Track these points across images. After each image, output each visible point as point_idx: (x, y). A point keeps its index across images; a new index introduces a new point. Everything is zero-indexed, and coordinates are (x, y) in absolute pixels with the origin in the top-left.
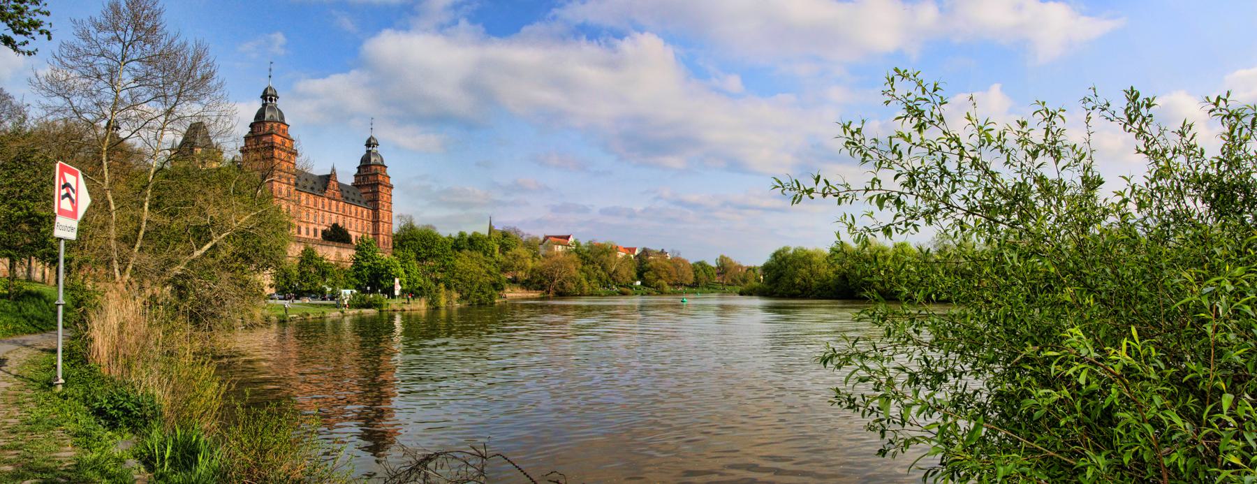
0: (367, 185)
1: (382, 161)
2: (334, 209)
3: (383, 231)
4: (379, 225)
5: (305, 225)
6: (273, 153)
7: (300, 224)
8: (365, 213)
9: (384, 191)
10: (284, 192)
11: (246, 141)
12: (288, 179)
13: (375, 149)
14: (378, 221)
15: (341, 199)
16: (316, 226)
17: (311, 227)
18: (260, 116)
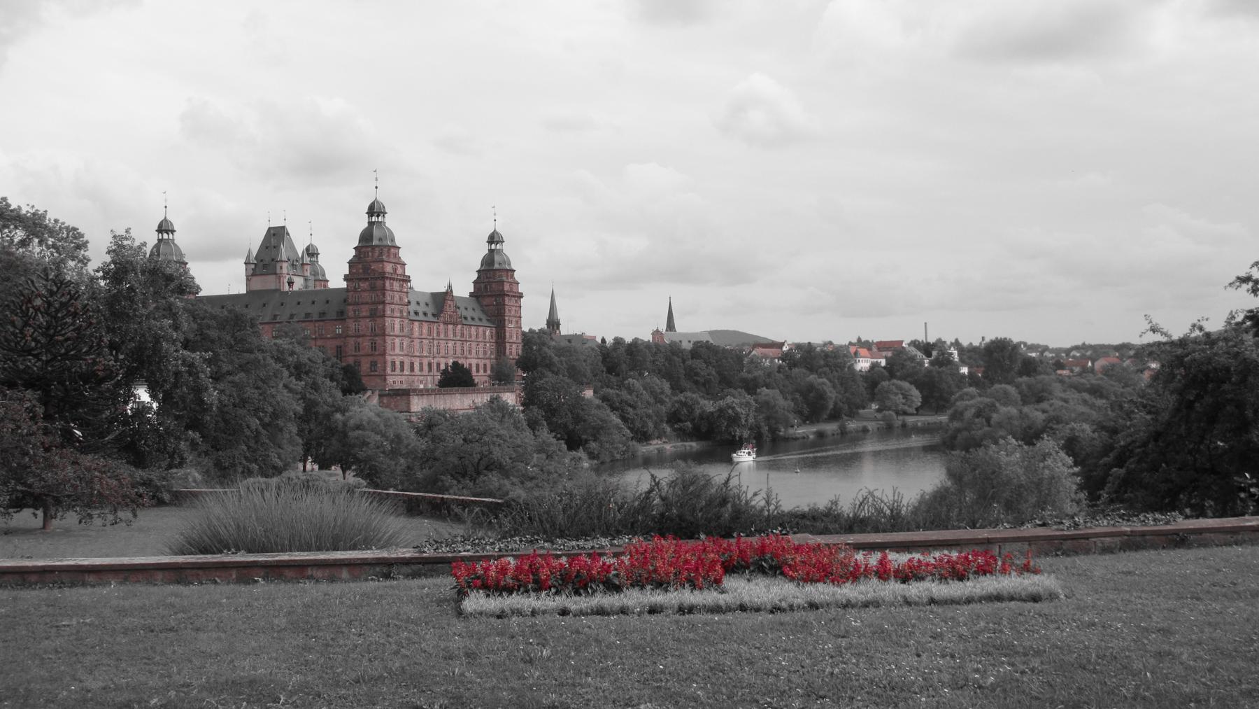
0: (489, 296)
2: (451, 335)
3: (511, 353)
5: (418, 359)
6: (384, 285)
7: (413, 359)
8: (488, 333)
10: (397, 327)
11: (350, 267)
12: (401, 312)
13: (498, 247)
14: (505, 343)
17: (425, 362)
18: (366, 237)
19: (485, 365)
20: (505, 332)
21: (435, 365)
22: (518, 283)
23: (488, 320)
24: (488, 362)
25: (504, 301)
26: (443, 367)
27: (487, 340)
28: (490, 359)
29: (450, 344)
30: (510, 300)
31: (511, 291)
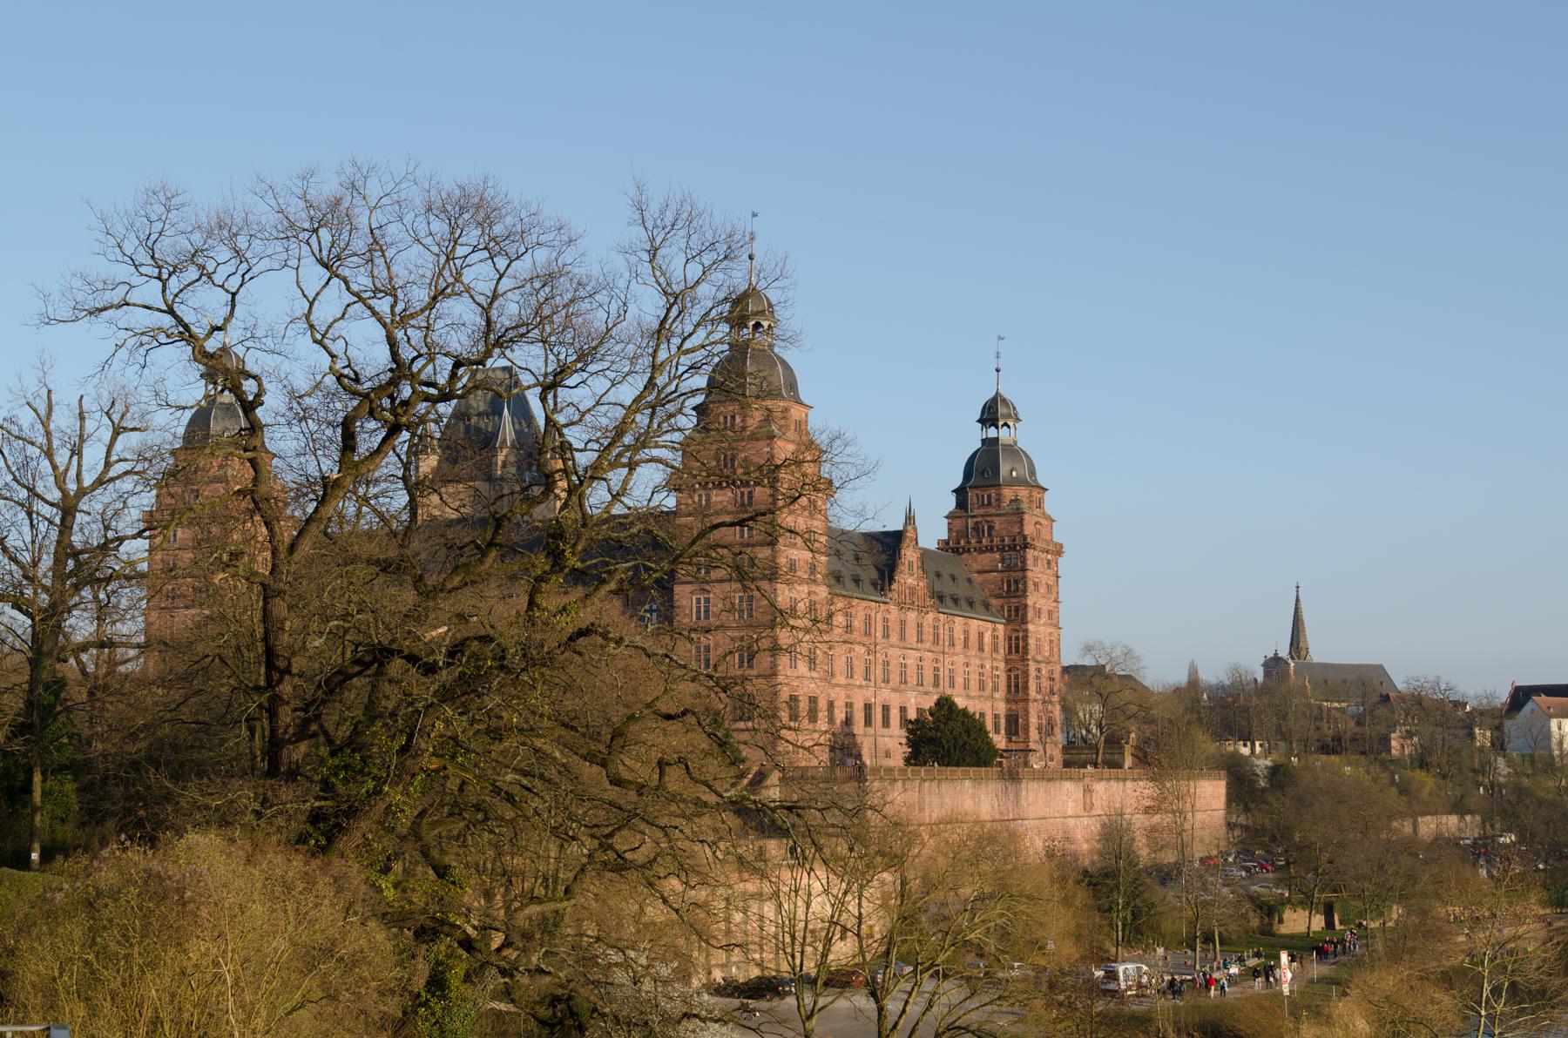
1: (1033, 472)
2: (911, 633)
4: (1026, 674)
8: (987, 638)
14: (1024, 660)
15: (929, 602)
16: (869, 693)
20: (1025, 638)
21: (879, 709)
25: (1024, 561)
26: (912, 715)
29: (911, 659)
30: (1036, 559)
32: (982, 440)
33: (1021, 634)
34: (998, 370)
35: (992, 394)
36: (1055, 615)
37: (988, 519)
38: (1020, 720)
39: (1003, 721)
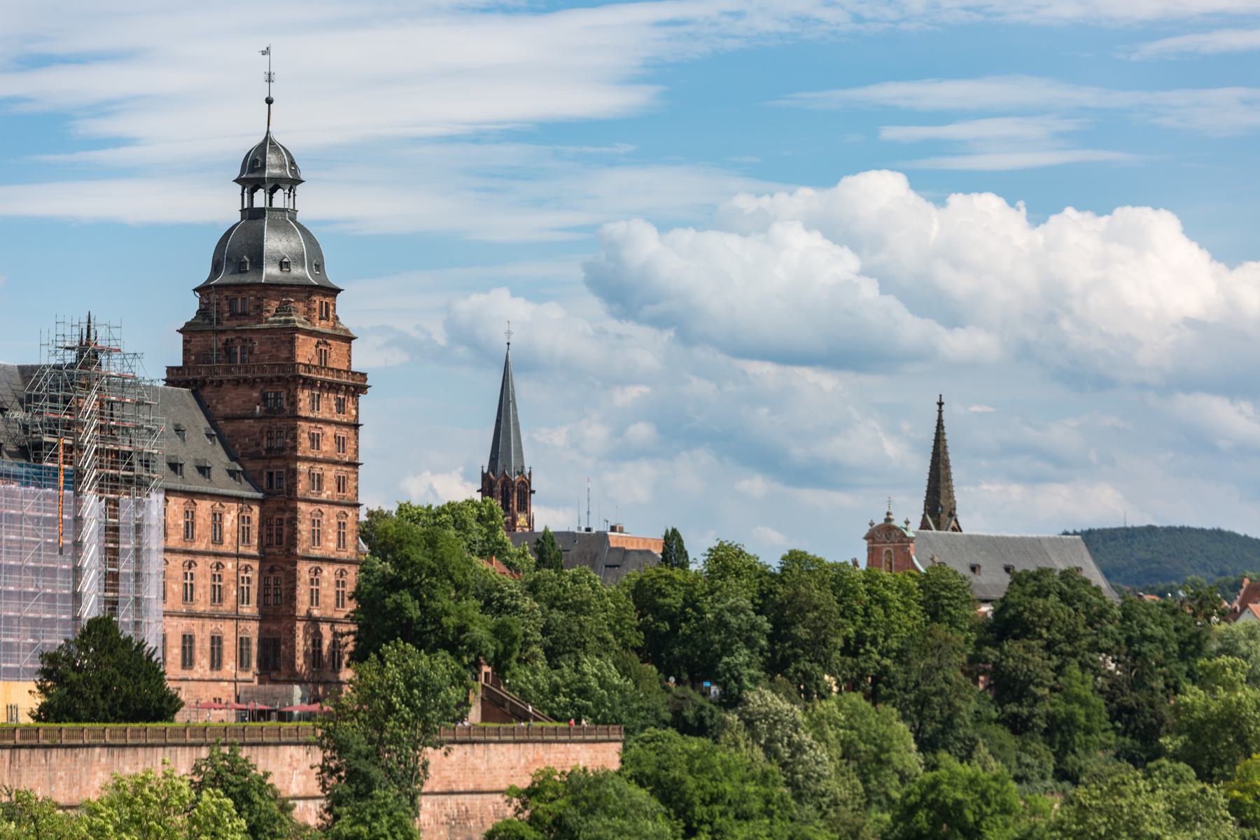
3: (315, 598)
9: (324, 413)
13: (280, 199)
14: (292, 559)
19: (216, 641)
20: (293, 521)
22: (348, 339)
23: (232, 473)
24: (228, 630)
25: (294, 403)
27: (228, 545)
28: (238, 618)
31: (323, 367)
32: (243, 210)
33: (287, 515)
34: (269, 101)
35: (261, 139)
36: (351, 484)
37: (244, 336)
38: (283, 647)
39: (254, 648)
